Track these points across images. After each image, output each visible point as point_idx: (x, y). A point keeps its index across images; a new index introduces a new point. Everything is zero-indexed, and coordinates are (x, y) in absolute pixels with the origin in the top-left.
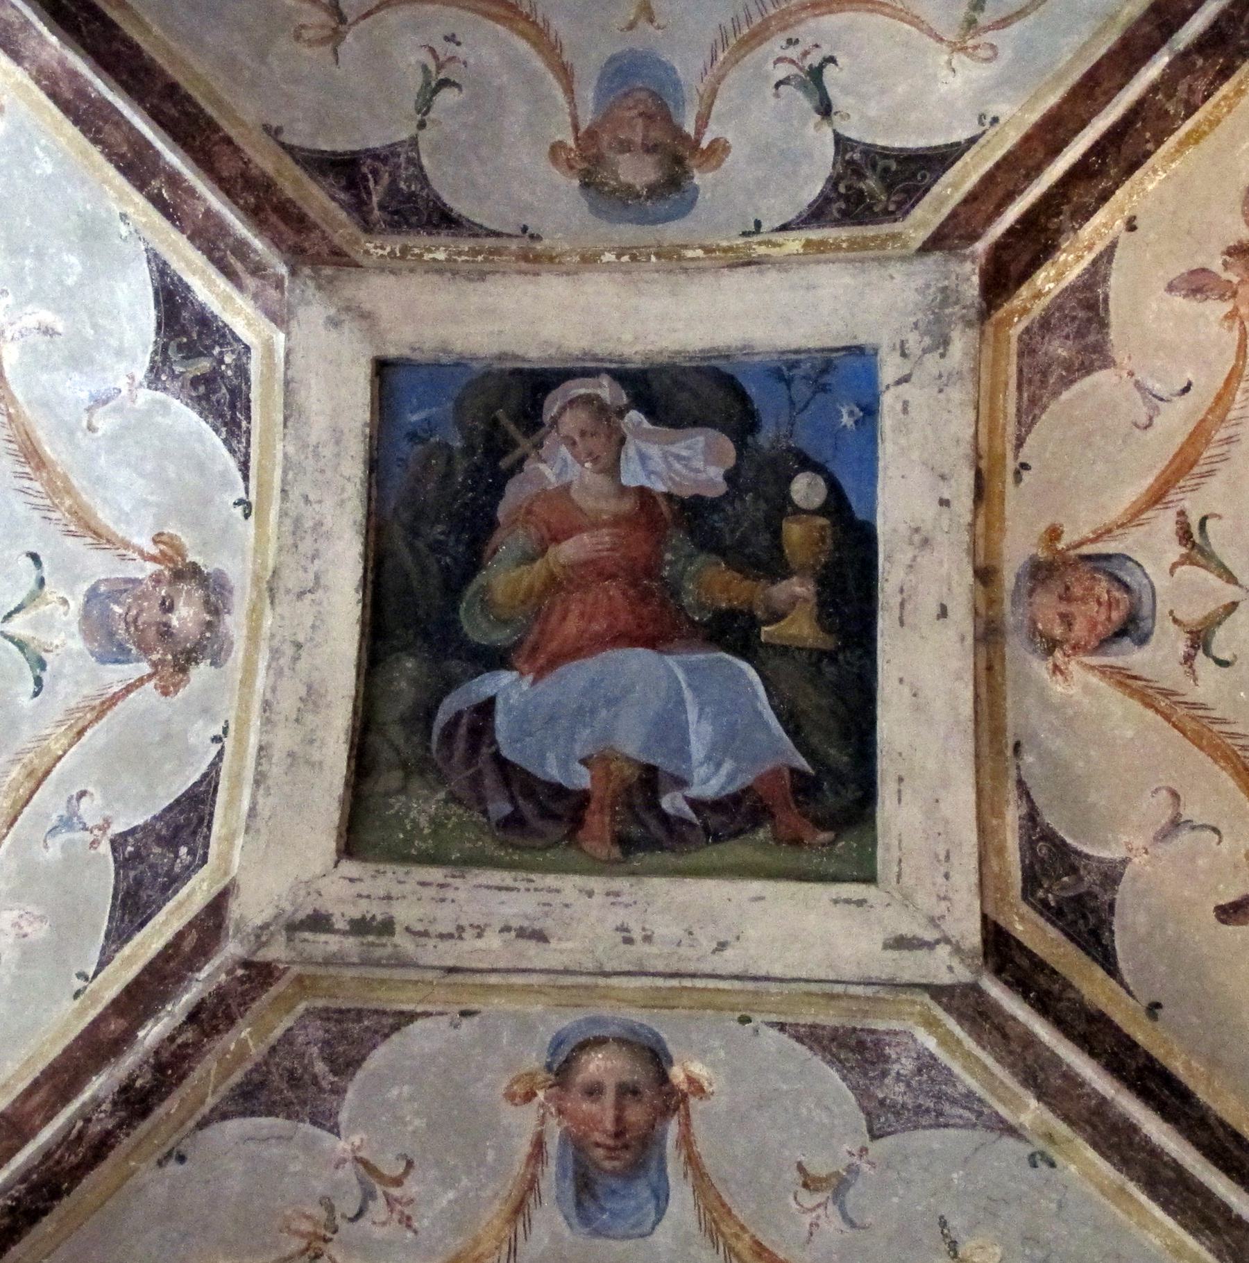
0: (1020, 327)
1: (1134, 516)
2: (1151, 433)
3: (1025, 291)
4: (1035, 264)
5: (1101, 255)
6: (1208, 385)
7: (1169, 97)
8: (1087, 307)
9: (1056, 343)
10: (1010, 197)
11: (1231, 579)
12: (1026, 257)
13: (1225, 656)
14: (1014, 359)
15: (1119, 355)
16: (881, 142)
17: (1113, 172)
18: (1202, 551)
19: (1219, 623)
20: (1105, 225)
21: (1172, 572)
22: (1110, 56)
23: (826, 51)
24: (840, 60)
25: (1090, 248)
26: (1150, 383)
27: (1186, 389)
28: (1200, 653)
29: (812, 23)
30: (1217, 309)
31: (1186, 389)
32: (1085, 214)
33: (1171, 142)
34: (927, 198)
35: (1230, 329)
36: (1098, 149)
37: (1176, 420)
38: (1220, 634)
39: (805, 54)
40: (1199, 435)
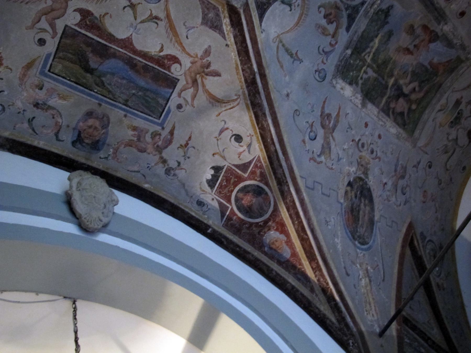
0: (220, 9)
1: (167, 9)
2: (182, 24)
3: (227, 15)
4: (231, 20)
5: (225, 36)
6: (186, 43)
7: (248, 67)
8: (216, 27)
9: (213, 15)
10: (247, 24)
11: (142, 22)
12: (234, 19)
13: (126, 9)
14: (215, 4)
15: (203, 27)
16: (271, 8)
17: (240, 48)
18: (151, 19)
19: (133, 13)
20: (231, 40)
21: (150, 10)
22: (261, 62)
23: (293, 10)
24: (290, 12)
25: (228, 34)
26: (193, 30)
27: (187, 37)
28: (129, 4)
29: (299, 12)
30: (200, 53)
31: (187, 37)
32: (235, 37)
33: (239, 63)
34: (256, 9)
35: (194, 54)
36: (247, 47)
37: (182, 31)
38: (131, 12)
39: (295, 6)
40: (176, 34)
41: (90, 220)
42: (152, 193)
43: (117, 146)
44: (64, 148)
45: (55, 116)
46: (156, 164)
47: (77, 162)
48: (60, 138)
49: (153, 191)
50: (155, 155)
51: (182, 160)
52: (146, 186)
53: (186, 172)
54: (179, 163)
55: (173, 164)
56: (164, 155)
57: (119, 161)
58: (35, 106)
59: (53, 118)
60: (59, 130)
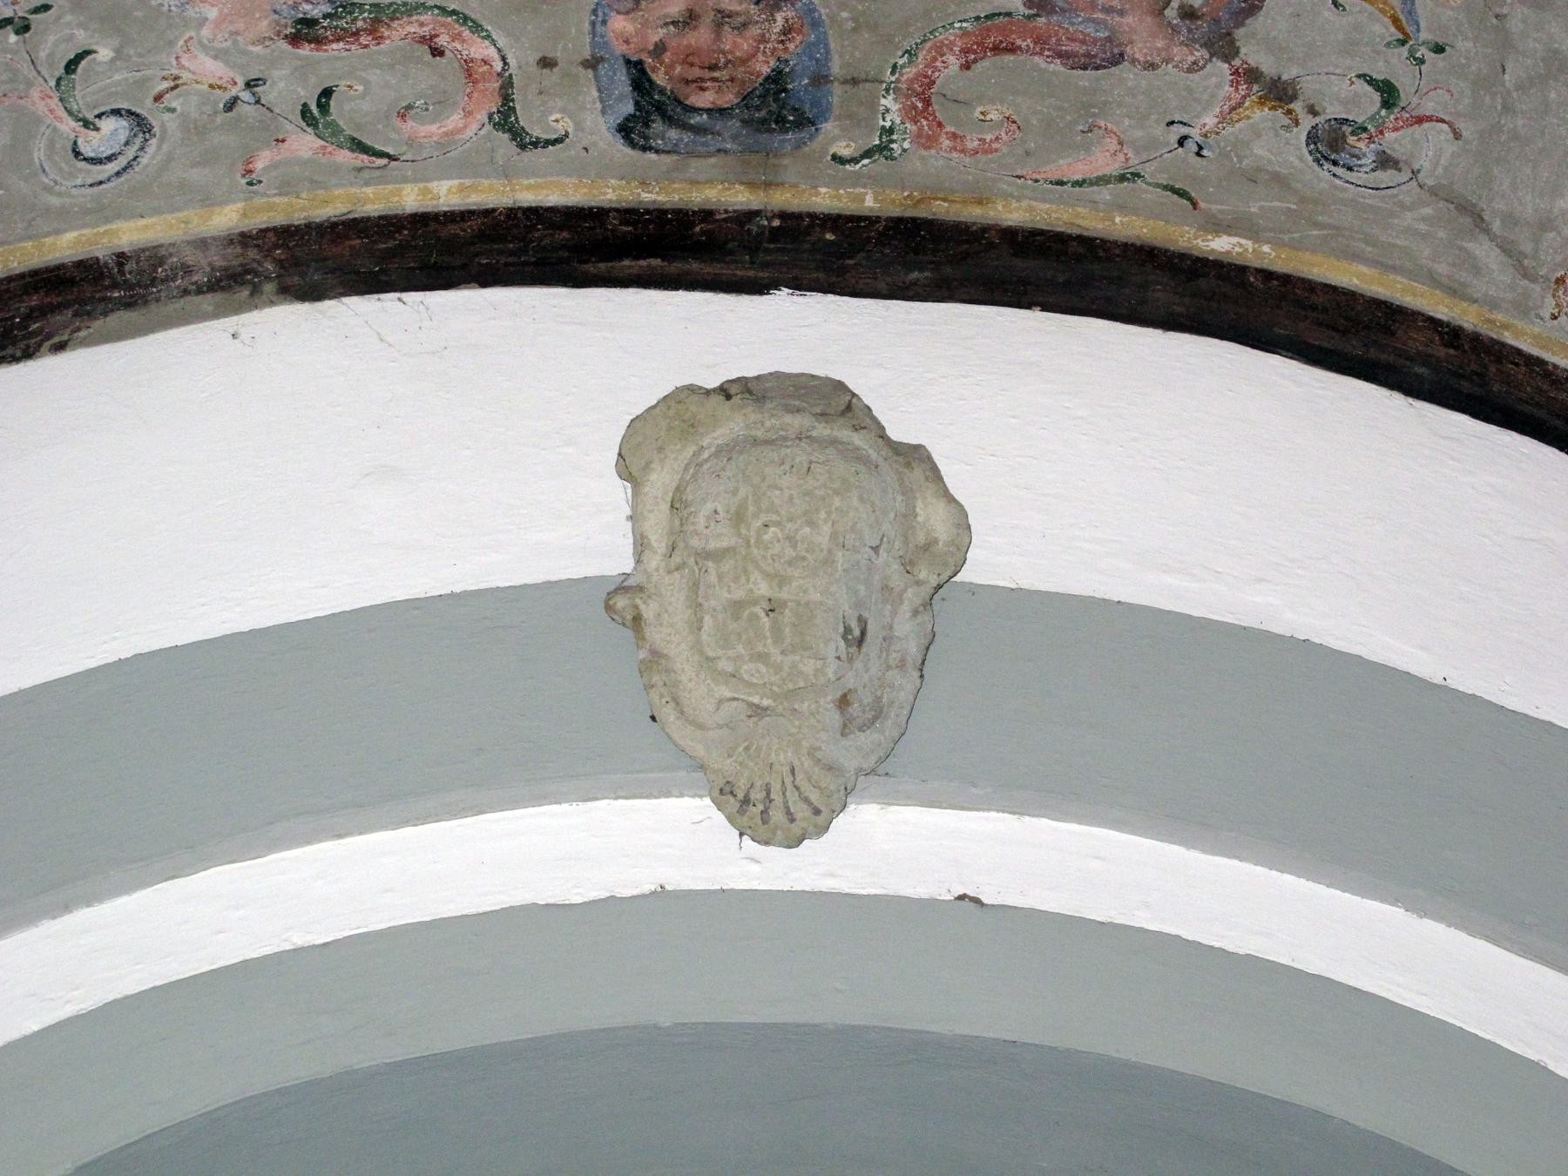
41: (757, 795)
42: (1286, 279)
43: (910, 72)
44: (588, 165)
45: (443, 41)
46: (1223, 119)
47: (707, 215)
48: (537, 132)
49: (1280, 267)
50: (1194, 68)
51: (1394, 66)
52: (1221, 245)
53: (1457, 135)
54: (1388, 93)
55: (1342, 96)
56: (1252, 53)
57: (972, 144)
58: (295, 40)
59: (437, 52)
60: (506, 98)
